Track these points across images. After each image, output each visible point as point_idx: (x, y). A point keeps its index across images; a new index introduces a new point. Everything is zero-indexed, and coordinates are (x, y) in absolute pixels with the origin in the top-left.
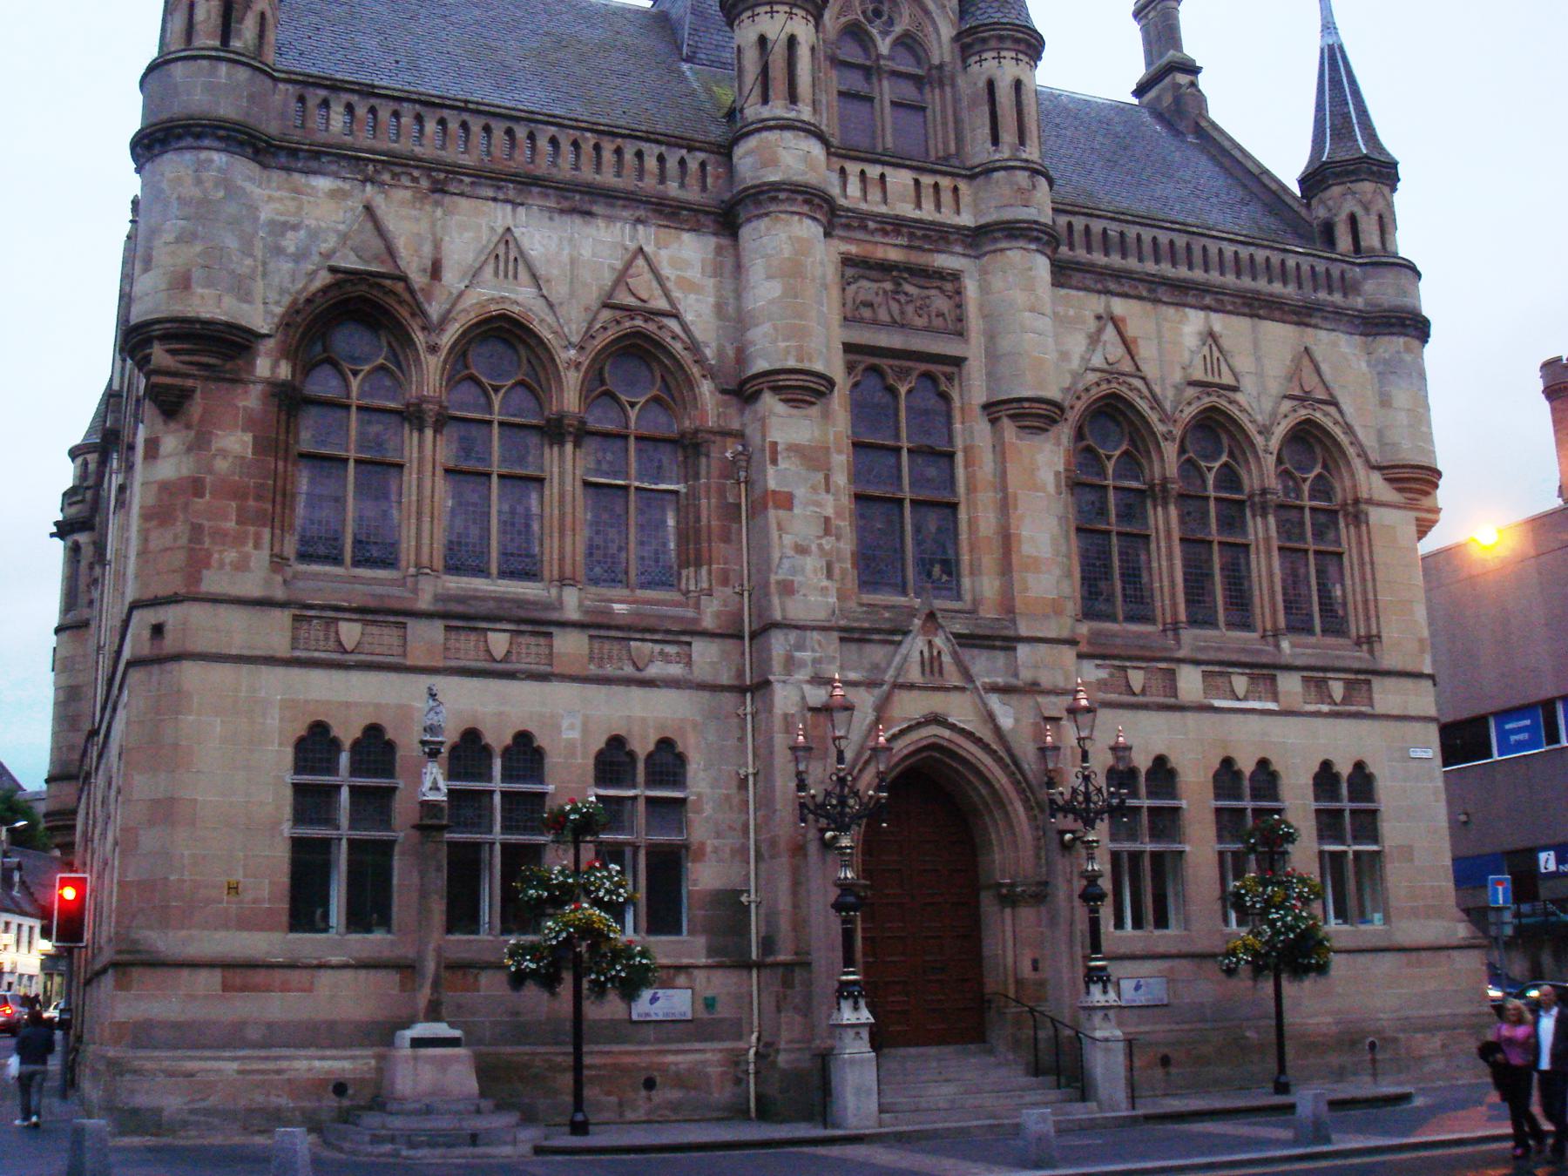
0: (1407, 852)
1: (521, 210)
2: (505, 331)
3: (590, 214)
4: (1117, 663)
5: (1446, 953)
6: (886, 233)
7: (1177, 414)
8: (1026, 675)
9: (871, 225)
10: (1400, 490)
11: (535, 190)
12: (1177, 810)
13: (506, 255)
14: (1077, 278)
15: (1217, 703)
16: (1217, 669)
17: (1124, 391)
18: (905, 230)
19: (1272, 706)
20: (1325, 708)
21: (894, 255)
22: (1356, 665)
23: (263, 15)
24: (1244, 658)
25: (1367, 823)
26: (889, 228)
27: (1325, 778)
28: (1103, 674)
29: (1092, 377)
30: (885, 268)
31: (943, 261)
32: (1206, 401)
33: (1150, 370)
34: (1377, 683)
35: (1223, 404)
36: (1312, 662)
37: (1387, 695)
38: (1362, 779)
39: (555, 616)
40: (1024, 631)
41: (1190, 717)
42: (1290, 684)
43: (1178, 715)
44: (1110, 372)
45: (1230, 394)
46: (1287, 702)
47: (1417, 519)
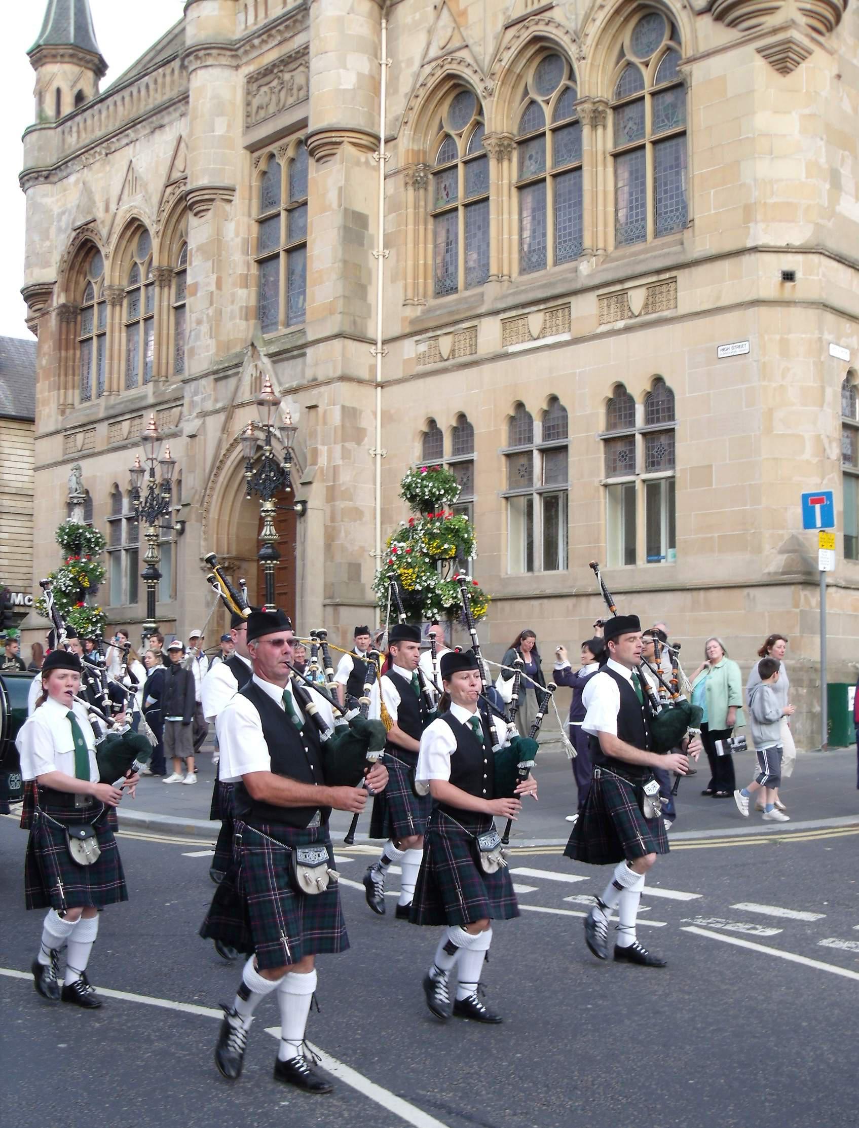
0: (703, 474)
1: (138, 142)
2: (135, 227)
3: (161, 126)
4: (431, 334)
5: (746, 591)
6: (264, 42)
7: (497, 67)
8: (309, 374)
9: (256, 42)
10: (733, 24)
11: (139, 126)
12: (471, 461)
13: (131, 179)
15: (512, 349)
16: (513, 313)
17: (454, 68)
18: (273, 32)
19: (566, 337)
20: (620, 324)
21: (271, 56)
22: (659, 265)
23: (58, 91)
24: (540, 294)
25: (662, 445)
26: (264, 37)
27: (619, 402)
28: (423, 348)
29: (428, 69)
30: (267, 71)
31: (298, 41)
32: (526, 36)
33: (473, 34)
34: (682, 276)
35: (541, 29)
36: (621, 274)
37: (693, 290)
38: (661, 398)
39: (144, 404)
40: (311, 337)
41: (487, 368)
42: (585, 308)
43: (474, 370)
44: (447, 54)
45: (547, 15)
46: (579, 329)
47: (759, 51)
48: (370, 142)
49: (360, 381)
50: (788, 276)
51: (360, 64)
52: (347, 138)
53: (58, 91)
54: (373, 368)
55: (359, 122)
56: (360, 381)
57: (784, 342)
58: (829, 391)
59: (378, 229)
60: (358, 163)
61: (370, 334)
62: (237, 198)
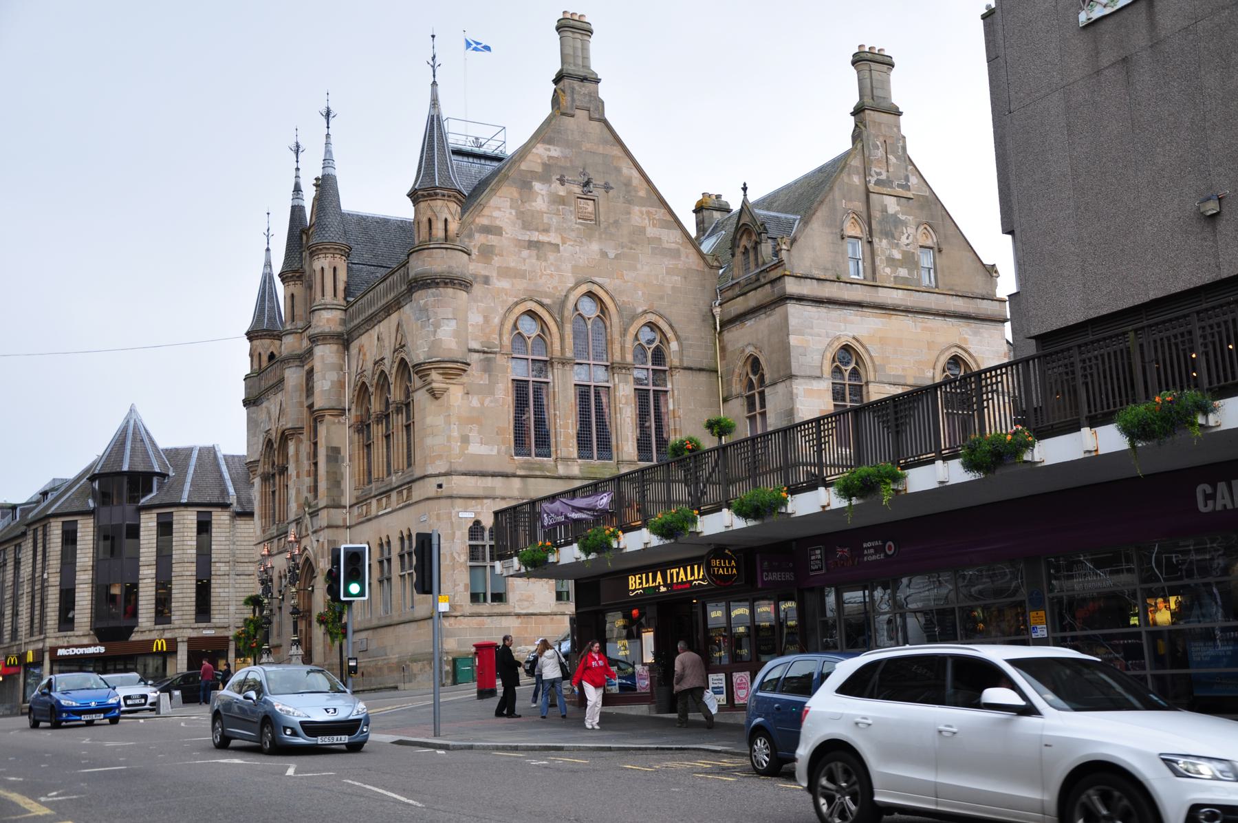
14: (355, 334)
37: (419, 491)
48: (342, 412)
49: (337, 527)
50: (440, 486)
51: (333, 376)
52: (327, 413)
53: (446, 220)
54: (345, 520)
55: (333, 404)
56: (337, 527)
57: (438, 515)
58: (458, 534)
59: (345, 453)
60: (334, 423)
61: (343, 503)
62: (305, 431)
